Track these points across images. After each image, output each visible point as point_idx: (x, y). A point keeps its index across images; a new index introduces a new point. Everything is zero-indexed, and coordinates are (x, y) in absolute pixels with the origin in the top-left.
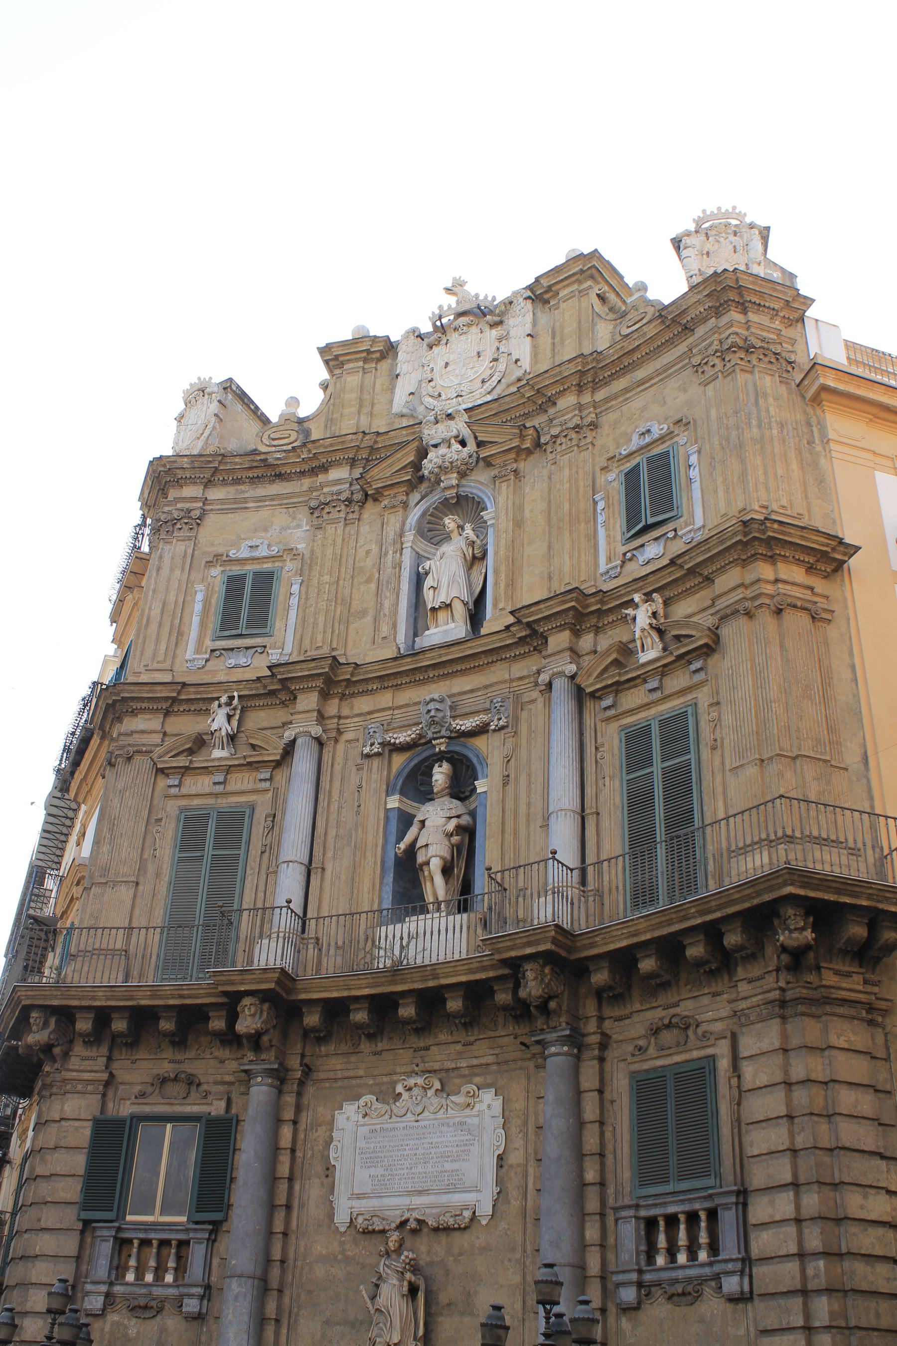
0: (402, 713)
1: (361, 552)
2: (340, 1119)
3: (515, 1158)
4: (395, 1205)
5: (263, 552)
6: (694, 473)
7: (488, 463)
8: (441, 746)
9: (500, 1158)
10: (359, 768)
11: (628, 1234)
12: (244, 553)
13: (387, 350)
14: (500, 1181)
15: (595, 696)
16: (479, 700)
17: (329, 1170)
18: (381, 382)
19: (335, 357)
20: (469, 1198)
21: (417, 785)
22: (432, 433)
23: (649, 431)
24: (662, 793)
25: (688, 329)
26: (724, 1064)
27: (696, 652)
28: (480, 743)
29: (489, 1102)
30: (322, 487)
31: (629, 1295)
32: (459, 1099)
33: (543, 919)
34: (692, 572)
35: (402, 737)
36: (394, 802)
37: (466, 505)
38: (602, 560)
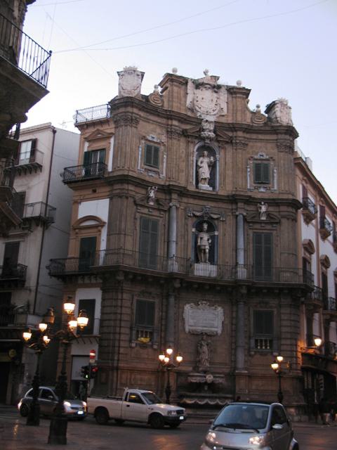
0: (197, 207)
1: (181, 151)
2: (185, 308)
3: (226, 322)
4: (199, 329)
5: (155, 140)
6: (275, 175)
7: (218, 141)
8: (206, 219)
9: (223, 323)
10: (186, 218)
11: (253, 342)
12: (150, 138)
13: (184, 82)
14: (223, 327)
15: (249, 222)
16: (215, 210)
17: (183, 319)
18: (182, 92)
20: (216, 329)
21: (200, 229)
22: (206, 126)
23: (262, 156)
24: (262, 252)
25: (277, 134)
26: (275, 313)
27: (273, 221)
28: (216, 222)
29: (220, 310)
30: (171, 125)
31: (253, 353)
32: (214, 308)
34: (277, 203)
35: (198, 214)
36: (194, 230)
37: (212, 152)
38: (249, 185)
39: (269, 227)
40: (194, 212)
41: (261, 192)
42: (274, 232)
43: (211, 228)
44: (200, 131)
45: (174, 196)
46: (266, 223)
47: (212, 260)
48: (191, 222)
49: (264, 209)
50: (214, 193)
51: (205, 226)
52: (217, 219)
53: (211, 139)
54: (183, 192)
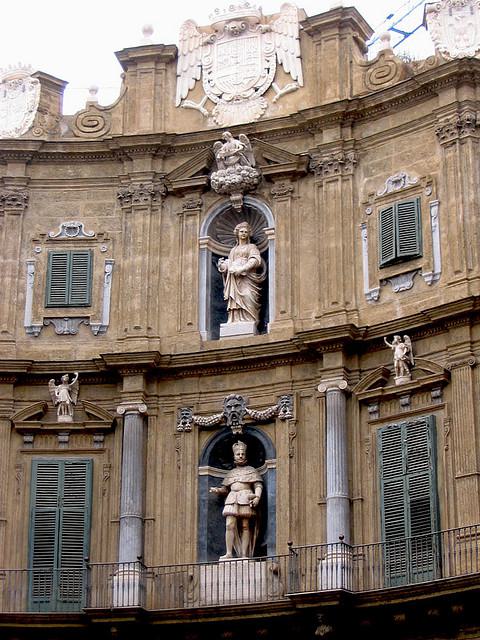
19: (130, 60)
21: (220, 457)
33: (334, 587)
35: (208, 420)
39: (422, 402)
40: (198, 419)
41: (399, 303)
42: (441, 415)
43: (256, 456)
44: (206, 171)
45: (133, 384)
46: (413, 393)
47: (259, 552)
48: (194, 445)
49: (399, 350)
50: (261, 339)
51: (239, 449)
52: (271, 420)
53: (249, 189)
54: (159, 371)
